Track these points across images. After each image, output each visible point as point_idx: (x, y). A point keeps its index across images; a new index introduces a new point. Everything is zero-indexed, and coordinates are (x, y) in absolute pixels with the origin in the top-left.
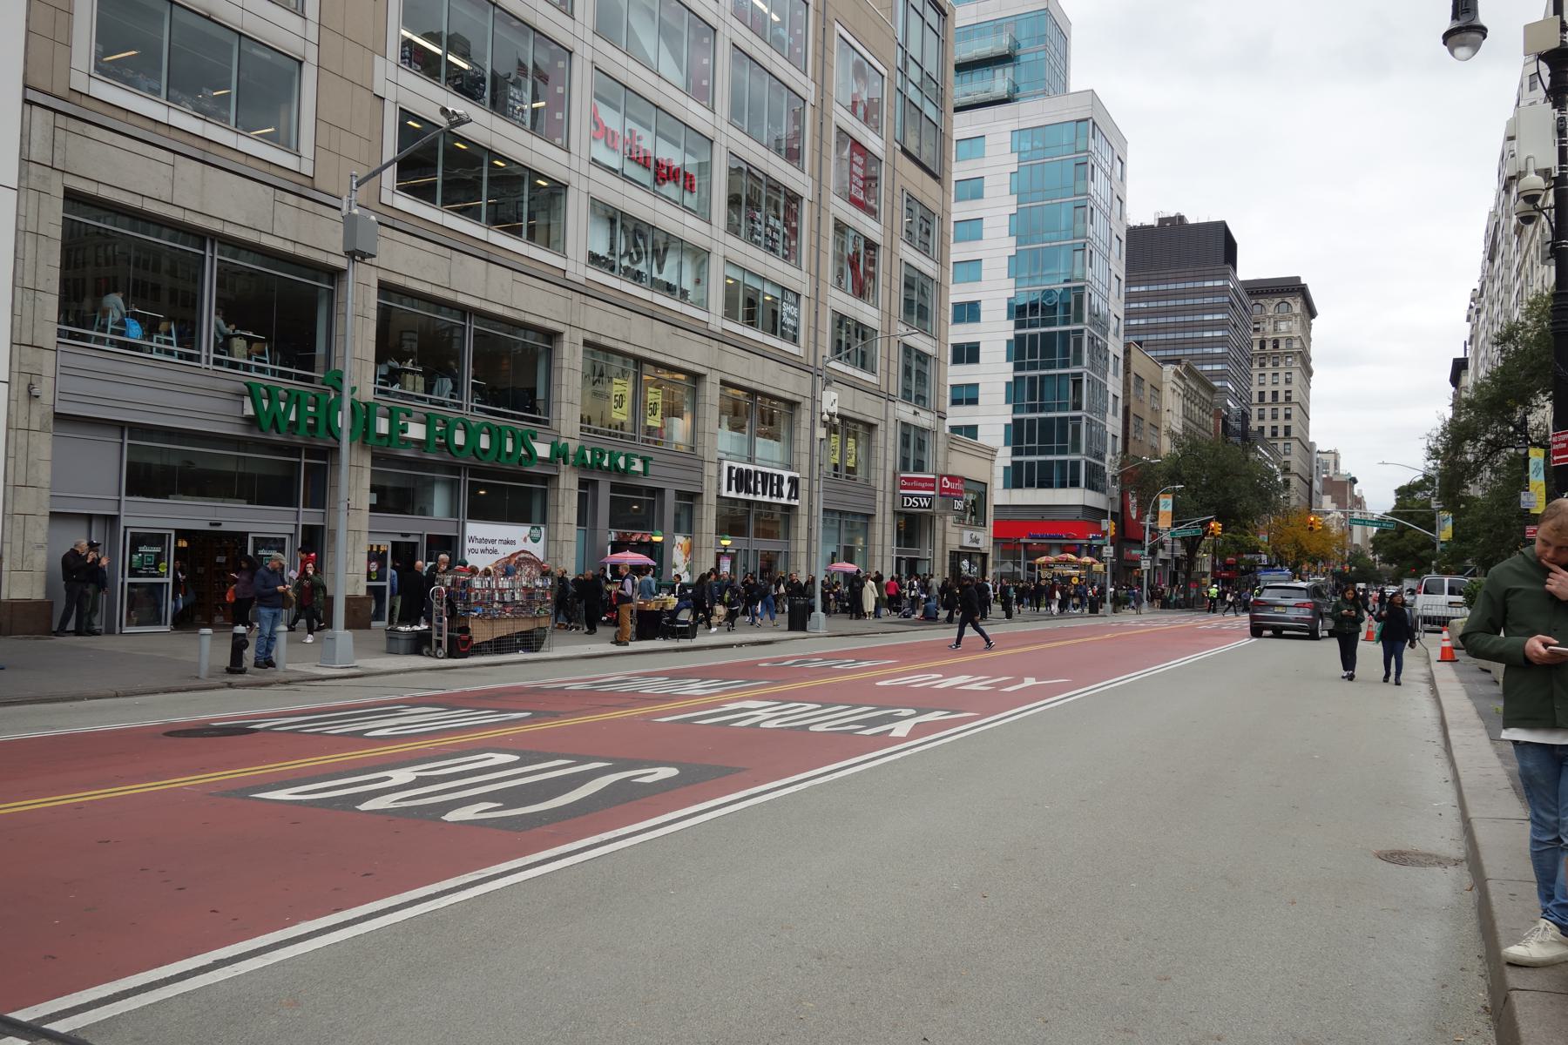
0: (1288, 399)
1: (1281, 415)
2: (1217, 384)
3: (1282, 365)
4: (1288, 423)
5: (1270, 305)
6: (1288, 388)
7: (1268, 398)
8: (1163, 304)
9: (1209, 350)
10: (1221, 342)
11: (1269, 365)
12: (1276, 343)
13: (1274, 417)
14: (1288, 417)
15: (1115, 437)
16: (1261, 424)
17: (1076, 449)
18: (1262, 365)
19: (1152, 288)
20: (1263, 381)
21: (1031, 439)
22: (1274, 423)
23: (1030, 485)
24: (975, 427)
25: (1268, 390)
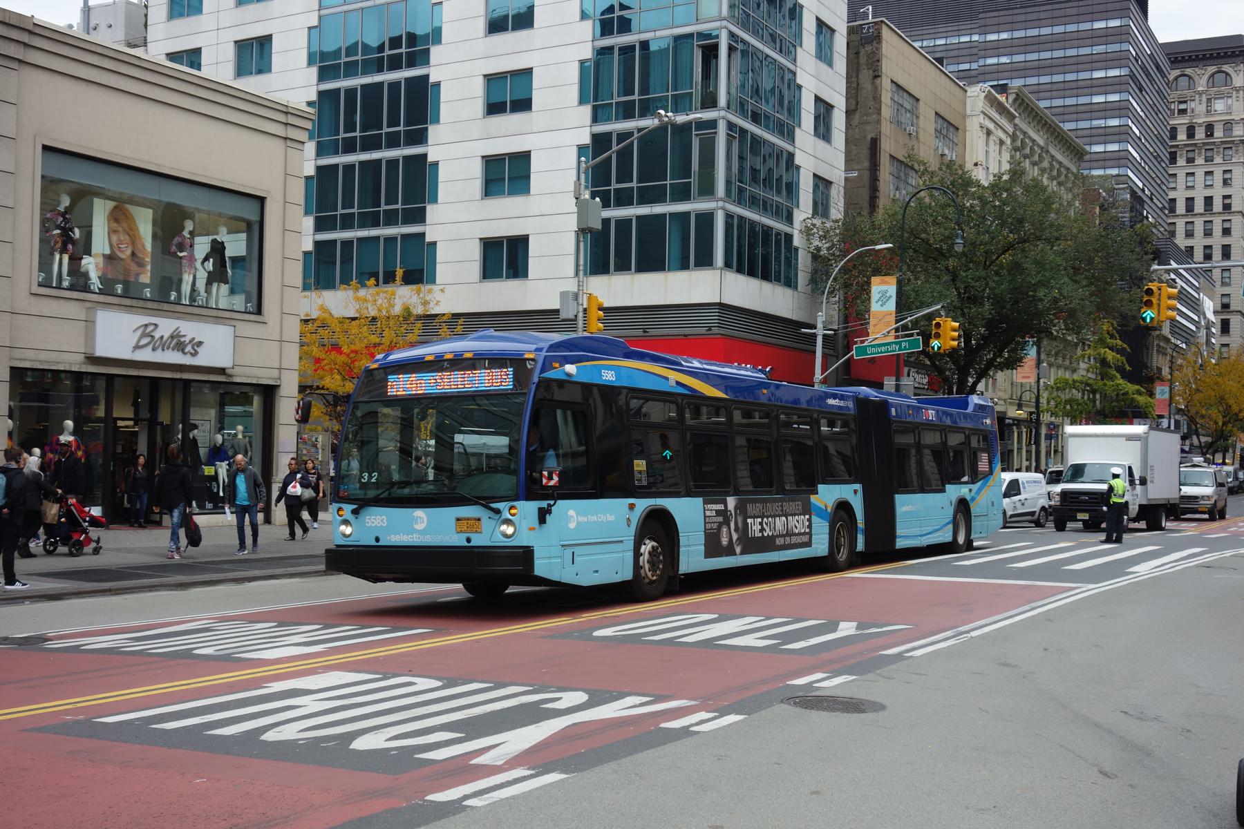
0: (1227, 207)
1: (1217, 229)
2: (1043, 104)
3: (1218, 160)
4: (1226, 241)
5: (1201, 76)
6: (1227, 191)
7: (1199, 206)
8: (1034, 56)
9: (1101, 123)
10: (1122, 109)
11: (1200, 161)
12: (1210, 128)
13: (1208, 233)
14: (1226, 232)
15: (822, 183)
16: (1189, 242)
17: (707, 189)
18: (1190, 161)
19: (1017, 34)
20: (1190, 183)
21: (624, 176)
22: (1208, 242)
23: (623, 266)
24: (525, 157)
25: (1199, 195)
